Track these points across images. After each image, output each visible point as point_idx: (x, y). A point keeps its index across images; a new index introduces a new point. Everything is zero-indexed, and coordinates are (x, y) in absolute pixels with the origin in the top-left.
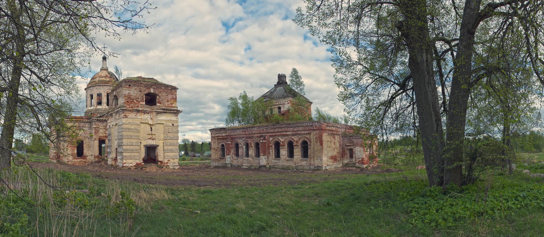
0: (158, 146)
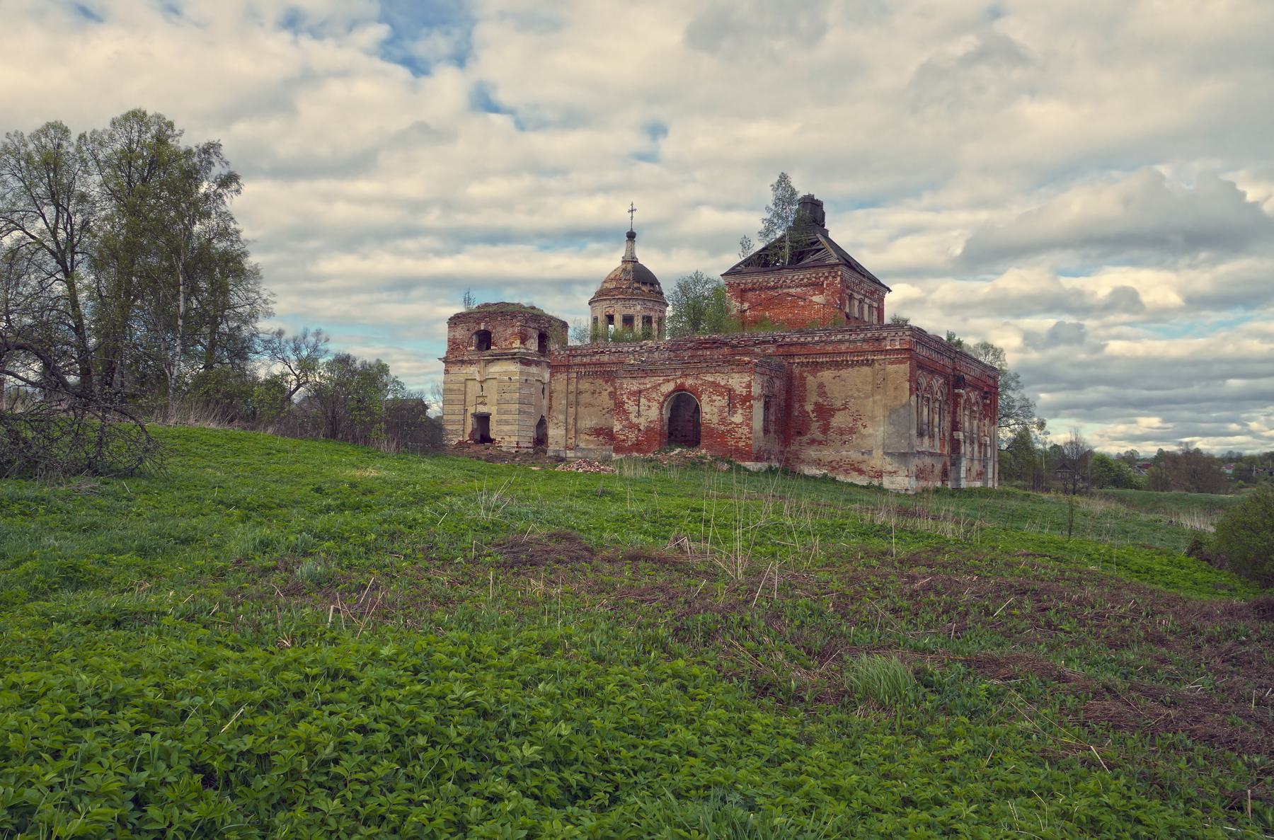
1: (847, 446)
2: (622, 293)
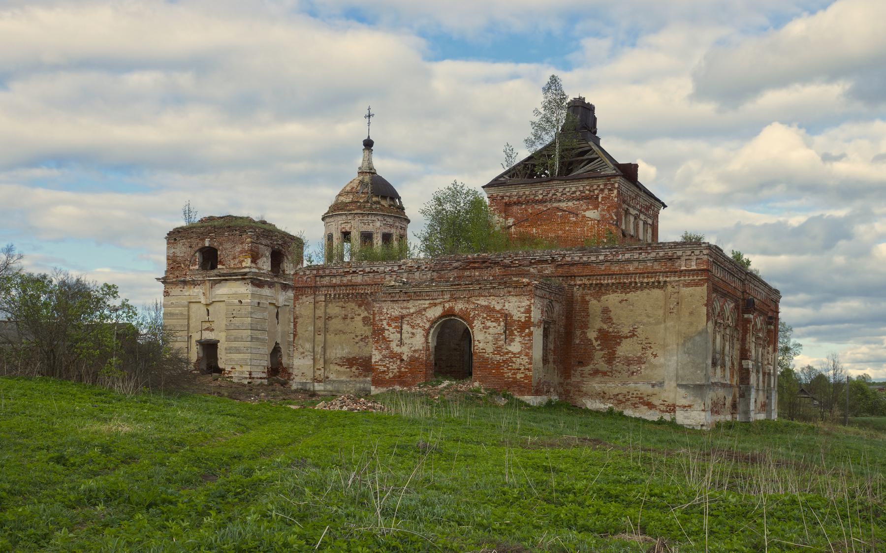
0: (218, 341)
1: (635, 377)
2: (359, 208)
